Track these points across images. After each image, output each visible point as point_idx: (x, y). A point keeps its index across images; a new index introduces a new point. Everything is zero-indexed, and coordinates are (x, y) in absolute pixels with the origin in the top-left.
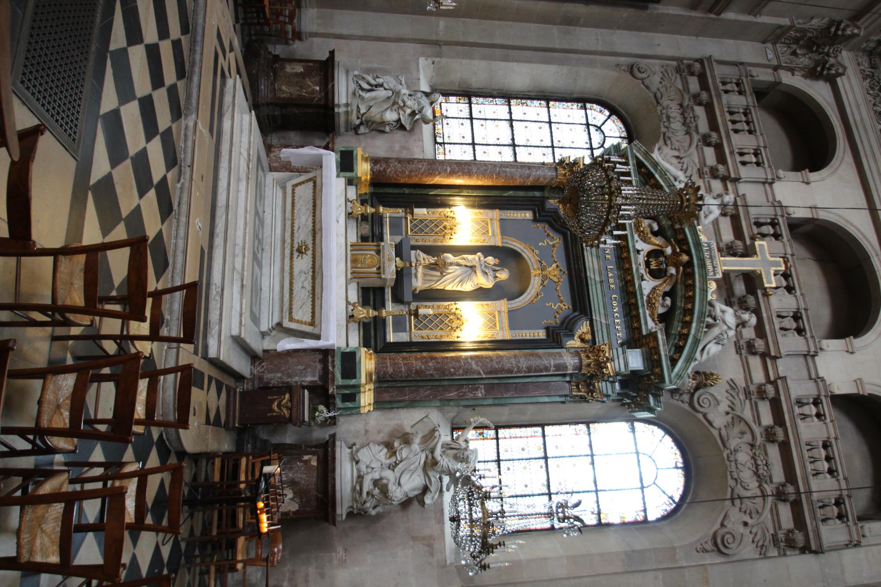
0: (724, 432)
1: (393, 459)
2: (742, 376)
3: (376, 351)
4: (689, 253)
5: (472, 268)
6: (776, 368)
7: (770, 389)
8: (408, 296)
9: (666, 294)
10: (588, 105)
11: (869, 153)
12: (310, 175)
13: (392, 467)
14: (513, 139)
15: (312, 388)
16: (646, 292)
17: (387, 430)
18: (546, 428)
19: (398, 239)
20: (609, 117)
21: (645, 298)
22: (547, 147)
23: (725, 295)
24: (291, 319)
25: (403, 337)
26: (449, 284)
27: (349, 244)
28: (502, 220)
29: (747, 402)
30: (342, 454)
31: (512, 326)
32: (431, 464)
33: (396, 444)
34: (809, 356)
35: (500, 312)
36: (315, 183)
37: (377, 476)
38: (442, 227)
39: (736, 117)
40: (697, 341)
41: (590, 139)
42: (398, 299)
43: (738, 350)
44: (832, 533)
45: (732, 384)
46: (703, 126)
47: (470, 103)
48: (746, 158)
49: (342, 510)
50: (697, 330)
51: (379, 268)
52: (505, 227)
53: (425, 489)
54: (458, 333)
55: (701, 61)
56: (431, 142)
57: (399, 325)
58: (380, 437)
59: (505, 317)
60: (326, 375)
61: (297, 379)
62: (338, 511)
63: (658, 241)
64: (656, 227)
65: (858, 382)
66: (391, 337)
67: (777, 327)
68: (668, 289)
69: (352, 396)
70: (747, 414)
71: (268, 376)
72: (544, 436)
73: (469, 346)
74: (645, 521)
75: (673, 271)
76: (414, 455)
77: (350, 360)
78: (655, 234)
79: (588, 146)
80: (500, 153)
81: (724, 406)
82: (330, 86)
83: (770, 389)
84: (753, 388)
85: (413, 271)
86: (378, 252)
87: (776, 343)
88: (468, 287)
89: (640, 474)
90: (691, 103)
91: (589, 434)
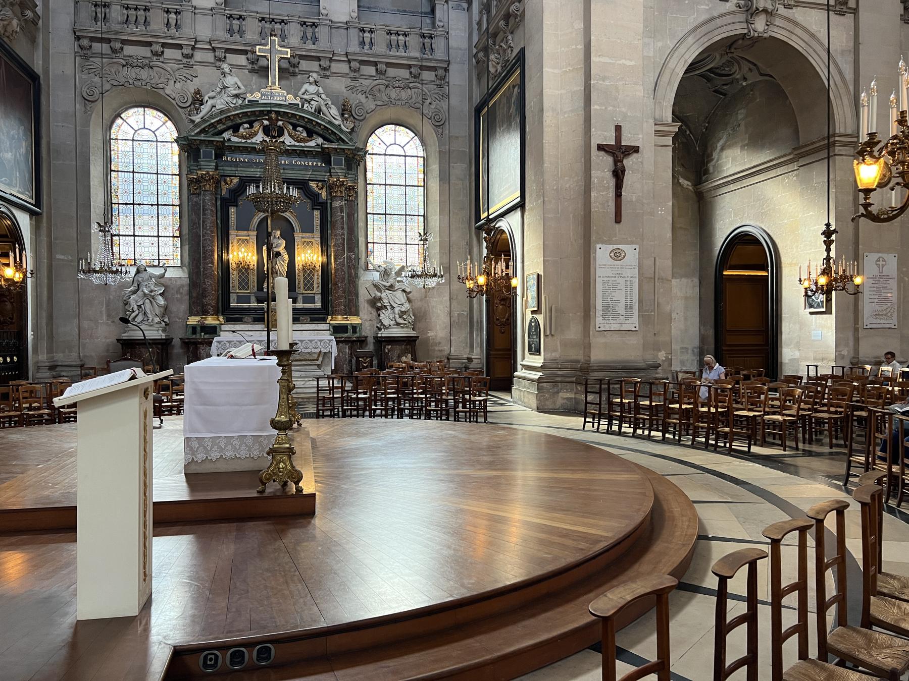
0: (379, 103)
2: (344, 79)
3: (328, 315)
4: (270, 112)
6: (340, 55)
7: (355, 65)
15: (351, 348)
16: (293, 143)
17: (370, 309)
19: (253, 299)
21: (297, 144)
23: (288, 75)
24: (317, 360)
25: (318, 298)
28: (238, 229)
30: (383, 333)
32: (391, 288)
33: (379, 305)
34: (333, 25)
37: (397, 316)
38: (244, 269)
40: (330, 123)
43: (328, 77)
44: (440, 54)
45: (351, 88)
46: (144, 52)
48: (173, 22)
49: (413, 334)
50: (323, 120)
52: (243, 226)
53: (404, 291)
56: (157, 269)
58: (374, 313)
59: (305, 235)
60: (346, 342)
63: (257, 125)
64: (246, 126)
66: (318, 305)
67: (313, 47)
68: (291, 127)
69: (354, 328)
70: (366, 82)
73: (325, 259)
75: (280, 123)
78: (251, 127)
84: (352, 74)
87: (324, 51)
88: (286, 257)
90: (121, 56)
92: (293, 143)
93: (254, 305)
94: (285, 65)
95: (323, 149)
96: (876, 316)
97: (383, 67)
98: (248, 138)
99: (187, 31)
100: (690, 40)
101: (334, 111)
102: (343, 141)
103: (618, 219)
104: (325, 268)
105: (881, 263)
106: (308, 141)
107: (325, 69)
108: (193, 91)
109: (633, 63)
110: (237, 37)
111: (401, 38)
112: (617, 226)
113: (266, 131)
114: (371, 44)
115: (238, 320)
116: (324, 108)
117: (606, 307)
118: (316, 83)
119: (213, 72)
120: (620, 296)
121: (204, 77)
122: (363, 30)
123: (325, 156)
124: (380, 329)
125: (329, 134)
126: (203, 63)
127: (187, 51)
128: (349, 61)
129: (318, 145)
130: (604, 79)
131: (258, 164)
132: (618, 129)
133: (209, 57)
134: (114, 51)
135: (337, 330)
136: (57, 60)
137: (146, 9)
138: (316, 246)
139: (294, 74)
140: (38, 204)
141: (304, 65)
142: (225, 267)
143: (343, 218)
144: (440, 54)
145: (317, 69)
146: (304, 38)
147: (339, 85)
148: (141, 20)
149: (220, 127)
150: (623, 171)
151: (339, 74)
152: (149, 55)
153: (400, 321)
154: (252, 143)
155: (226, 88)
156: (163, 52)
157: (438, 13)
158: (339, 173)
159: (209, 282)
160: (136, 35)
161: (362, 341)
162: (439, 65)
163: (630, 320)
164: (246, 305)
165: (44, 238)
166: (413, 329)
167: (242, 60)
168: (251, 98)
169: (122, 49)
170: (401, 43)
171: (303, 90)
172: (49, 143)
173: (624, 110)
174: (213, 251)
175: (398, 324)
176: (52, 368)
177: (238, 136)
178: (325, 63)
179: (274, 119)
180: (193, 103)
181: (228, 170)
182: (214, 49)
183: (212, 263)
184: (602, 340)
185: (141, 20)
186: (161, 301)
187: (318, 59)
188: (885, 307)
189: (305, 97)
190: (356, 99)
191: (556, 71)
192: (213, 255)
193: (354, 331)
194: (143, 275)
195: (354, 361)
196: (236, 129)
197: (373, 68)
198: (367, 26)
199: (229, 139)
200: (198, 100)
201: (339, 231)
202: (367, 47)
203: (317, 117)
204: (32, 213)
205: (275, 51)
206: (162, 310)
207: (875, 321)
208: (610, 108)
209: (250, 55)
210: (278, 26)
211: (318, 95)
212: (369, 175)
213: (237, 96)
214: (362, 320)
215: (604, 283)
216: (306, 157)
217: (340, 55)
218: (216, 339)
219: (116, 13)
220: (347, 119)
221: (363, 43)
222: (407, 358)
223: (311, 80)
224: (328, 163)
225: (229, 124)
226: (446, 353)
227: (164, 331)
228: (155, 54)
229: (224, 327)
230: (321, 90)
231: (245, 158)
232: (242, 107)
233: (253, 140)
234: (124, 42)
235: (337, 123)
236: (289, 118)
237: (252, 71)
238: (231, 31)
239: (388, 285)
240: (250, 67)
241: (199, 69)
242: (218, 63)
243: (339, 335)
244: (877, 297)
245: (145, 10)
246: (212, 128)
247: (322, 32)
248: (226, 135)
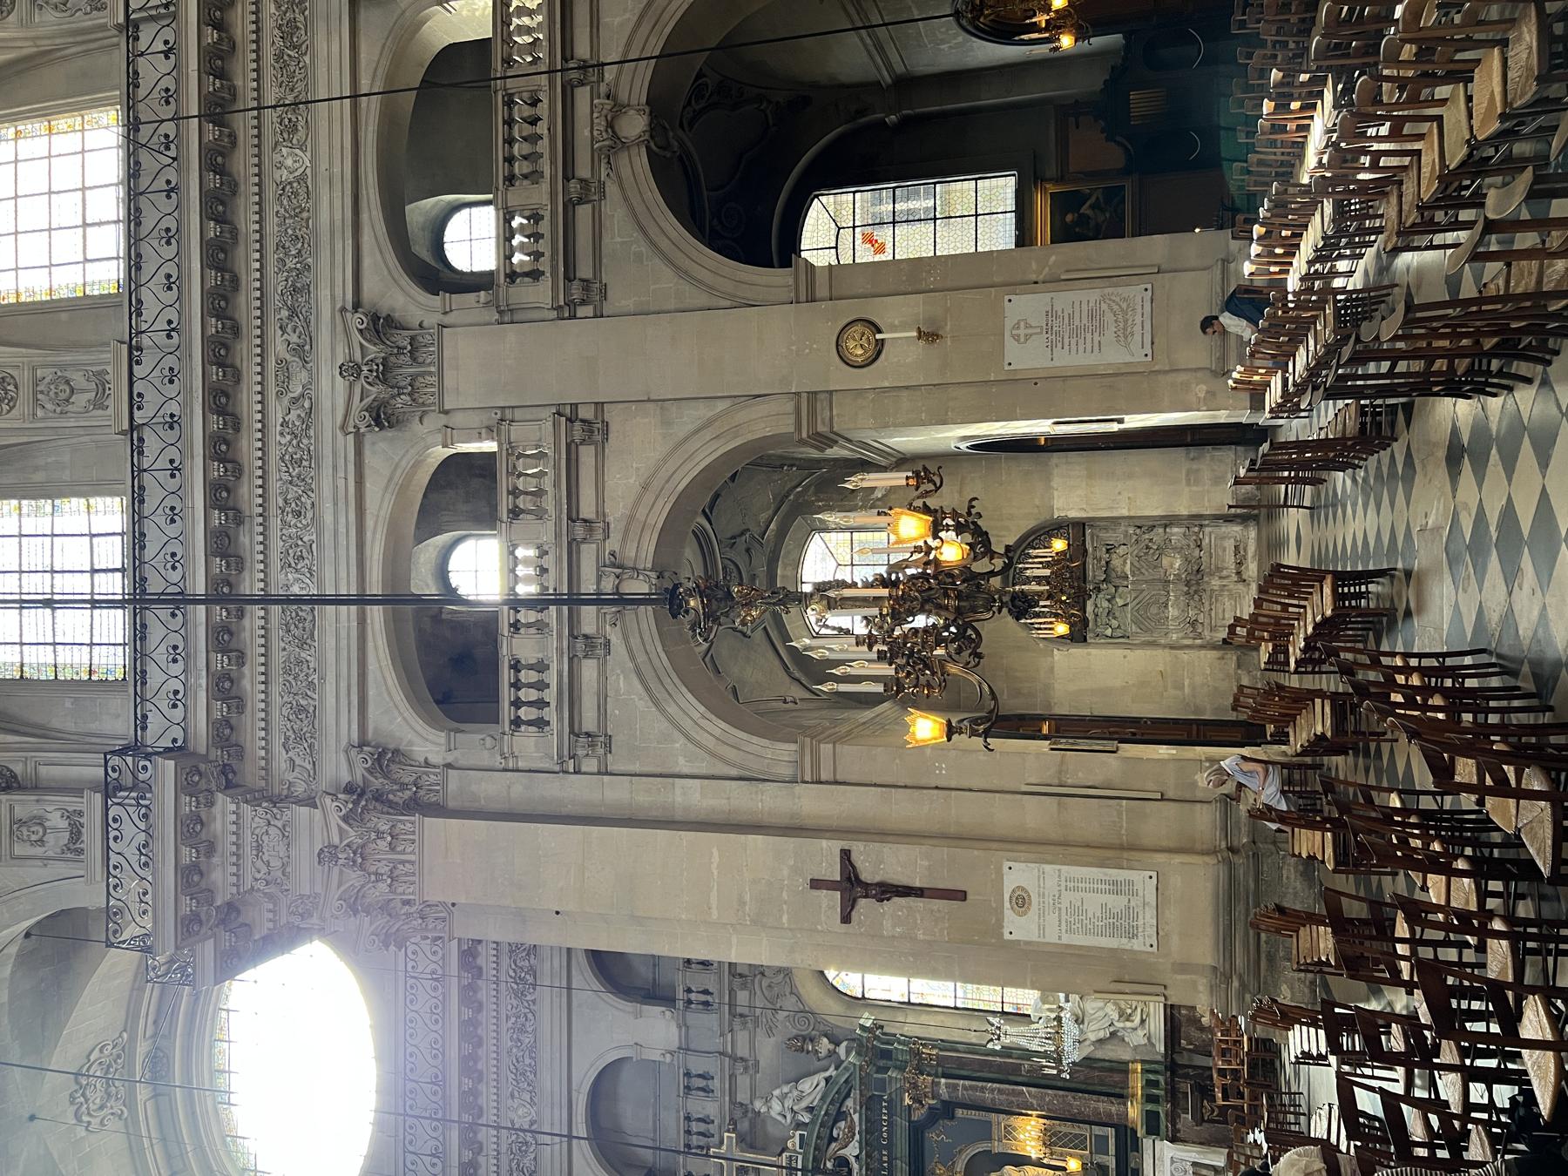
0: (788, 990)
9: (836, 1140)
21: (857, 1137)
25: (1097, 1130)
34: (685, 1049)
37: (1128, 1024)
45: (770, 1032)
65: (638, 1015)
66: (1111, 1132)
68: (833, 1145)
75: (829, 1165)
96: (1124, 335)
100: (672, 709)
103: (961, 896)
105: (1022, 332)
109: (715, 851)
112: (969, 897)
114: (706, 992)
117: (1113, 930)
120: (1094, 903)
130: (742, 903)
132: (816, 884)
150: (881, 885)
151: (752, 1047)
153: (1137, 1020)
163: (1138, 886)
171: (780, 1118)
173: (786, 872)
184: (1175, 941)
187: (732, 1076)
188: (1109, 317)
191: (734, 940)
207: (1138, 337)
208: (785, 895)
215: (1069, 931)
217: (725, 1043)
230: (777, 1092)
244: (1089, 336)
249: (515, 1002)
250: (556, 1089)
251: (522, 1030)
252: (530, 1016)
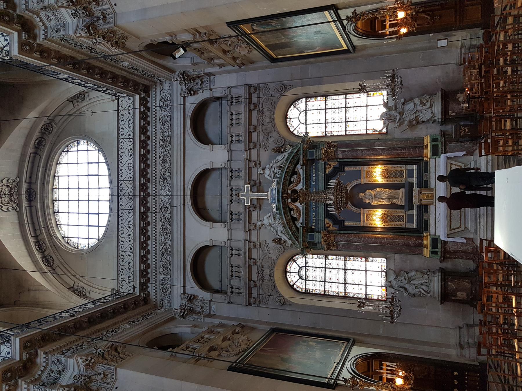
0: (273, 130)
1: (417, 115)
2: (261, 152)
3: (423, 160)
4: (282, 197)
5: (375, 197)
8: (407, 186)
10: (304, 291)
11: (179, 253)
12: (453, 231)
13: (417, 111)
14: (345, 273)
15: (450, 142)
16: (301, 184)
18: (344, 134)
19: (410, 212)
20: (294, 284)
21: (302, 181)
22: (328, 268)
25: (409, 167)
26: (386, 192)
27: (434, 204)
28: (360, 221)
29: (261, 142)
30: (438, 117)
31: (360, 172)
32: (401, 113)
33: (415, 122)
34: (230, 160)
35: (364, 178)
36: (450, 228)
37: (424, 107)
39: (237, 274)
40: (287, 160)
41: (306, 272)
42: (411, 185)
43: (260, 162)
44: (240, 92)
46: (254, 269)
47: (366, 294)
48: (237, 252)
49: (439, 94)
51: (421, 193)
52: (358, 217)
54: (385, 168)
55: (250, 304)
57: (411, 172)
58: (420, 126)
59: (362, 177)
60: (445, 145)
61: (458, 144)
62: (440, 94)
63: (291, 207)
66: (415, 167)
67: (243, 172)
68: (292, 185)
69: (433, 140)
70: (261, 138)
71: (471, 145)
72: (346, 131)
74: (307, 98)
75: (289, 192)
76: (408, 117)
77: (435, 152)
79: (307, 268)
80: (353, 265)
81: (271, 140)
82: (443, 283)
83: (252, 147)
84: (257, 147)
85: (404, 195)
86: (421, 200)
89: (306, 116)
90: (257, 282)
91: (326, 132)
92: (301, 184)
93: (415, 212)
94: (255, 188)
95: (303, 165)
97: (252, 127)
98: (300, 212)
99: (241, 245)
101: (280, 158)
102: (298, 151)
104: (386, 163)
106: (299, 174)
107: (255, 164)
108: (274, 244)
110: (242, 217)
111: (234, 117)
113: (294, 200)
115: (427, 223)
116: (278, 164)
118: (264, 169)
119: (262, 231)
121: (266, 236)
122: (232, 141)
123: (309, 163)
124: (434, 121)
125: (294, 161)
126: (258, 237)
127: (252, 246)
128: (250, 149)
129: (302, 168)
131: (316, 206)
133: (254, 233)
134: (255, 286)
135: (435, 152)
136: (264, 316)
137: (232, 266)
138: (369, 169)
139: (260, 183)
140: (348, 340)
141: (254, 177)
142: (386, 230)
143: (350, 151)
144: (240, 92)
145: (255, 169)
146: (239, 177)
147: (265, 155)
148: (237, 269)
149: (294, 229)
151: (258, 156)
152: (256, 267)
154: (303, 209)
155: (270, 225)
156: (254, 259)
157: (217, 94)
158: (318, 154)
159: (398, 241)
160: (245, 273)
161: (444, 134)
162: (248, 91)
164: (415, 218)
165: (368, 340)
166: (435, 94)
167: (254, 214)
168: (275, 210)
169: (254, 281)
170: (237, 117)
171: (269, 178)
172: (309, 328)
174: (376, 238)
175: (431, 106)
176: (461, 347)
177: (299, 218)
178: (252, 165)
179: (287, 196)
180: (281, 244)
181: (321, 225)
182: (249, 230)
183: (384, 238)
185: (237, 269)
186: (413, 274)
187: (250, 168)
189: (272, 176)
190: (272, 144)
192: (378, 238)
193: (437, 140)
194: (394, 283)
195: (461, 139)
196: (294, 219)
197: (253, 133)
198: (229, 139)
199: (301, 223)
200: (278, 241)
201: (359, 153)
202: (241, 138)
203: (284, 168)
204: (353, 344)
205: (247, 195)
206: (418, 273)
209: (251, 209)
210: (234, 192)
211: (270, 168)
212: (320, 134)
213: (274, 218)
214: (427, 135)
216: (310, 175)
218: (442, 238)
219: (235, 282)
220: (285, 150)
221: (239, 141)
222: (461, 97)
223: (262, 172)
224: (313, 161)
225: (291, 223)
226: (455, 66)
227: (434, 273)
228: (255, 264)
229: (432, 232)
230: (268, 166)
231: (312, 215)
232: (281, 215)
233: (301, 209)
234: (250, 280)
235: (287, 156)
236: (286, 186)
237: (260, 208)
238: (239, 220)
239: (399, 116)
240: (258, 210)
241: (262, 239)
242: (257, 228)
243: (440, 151)
245: (232, 267)
246: (295, 234)
247: (235, 166)
248: (299, 225)
249: (162, 150)
250: (179, 184)
251: (165, 162)
252: (168, 155)
